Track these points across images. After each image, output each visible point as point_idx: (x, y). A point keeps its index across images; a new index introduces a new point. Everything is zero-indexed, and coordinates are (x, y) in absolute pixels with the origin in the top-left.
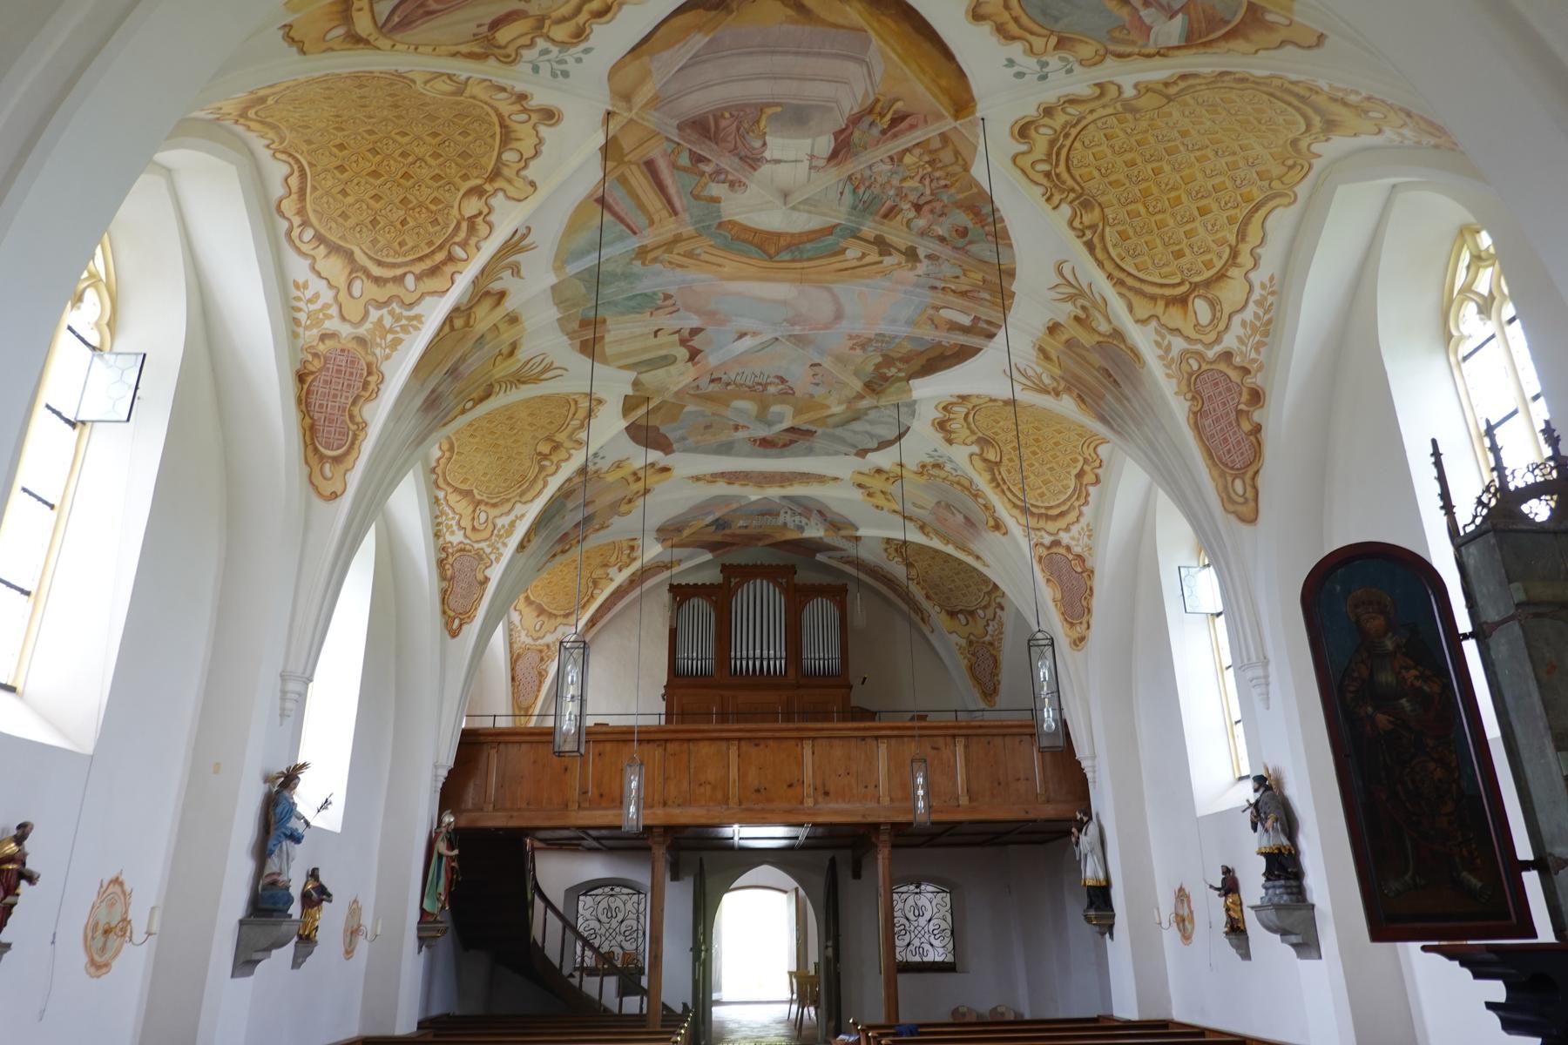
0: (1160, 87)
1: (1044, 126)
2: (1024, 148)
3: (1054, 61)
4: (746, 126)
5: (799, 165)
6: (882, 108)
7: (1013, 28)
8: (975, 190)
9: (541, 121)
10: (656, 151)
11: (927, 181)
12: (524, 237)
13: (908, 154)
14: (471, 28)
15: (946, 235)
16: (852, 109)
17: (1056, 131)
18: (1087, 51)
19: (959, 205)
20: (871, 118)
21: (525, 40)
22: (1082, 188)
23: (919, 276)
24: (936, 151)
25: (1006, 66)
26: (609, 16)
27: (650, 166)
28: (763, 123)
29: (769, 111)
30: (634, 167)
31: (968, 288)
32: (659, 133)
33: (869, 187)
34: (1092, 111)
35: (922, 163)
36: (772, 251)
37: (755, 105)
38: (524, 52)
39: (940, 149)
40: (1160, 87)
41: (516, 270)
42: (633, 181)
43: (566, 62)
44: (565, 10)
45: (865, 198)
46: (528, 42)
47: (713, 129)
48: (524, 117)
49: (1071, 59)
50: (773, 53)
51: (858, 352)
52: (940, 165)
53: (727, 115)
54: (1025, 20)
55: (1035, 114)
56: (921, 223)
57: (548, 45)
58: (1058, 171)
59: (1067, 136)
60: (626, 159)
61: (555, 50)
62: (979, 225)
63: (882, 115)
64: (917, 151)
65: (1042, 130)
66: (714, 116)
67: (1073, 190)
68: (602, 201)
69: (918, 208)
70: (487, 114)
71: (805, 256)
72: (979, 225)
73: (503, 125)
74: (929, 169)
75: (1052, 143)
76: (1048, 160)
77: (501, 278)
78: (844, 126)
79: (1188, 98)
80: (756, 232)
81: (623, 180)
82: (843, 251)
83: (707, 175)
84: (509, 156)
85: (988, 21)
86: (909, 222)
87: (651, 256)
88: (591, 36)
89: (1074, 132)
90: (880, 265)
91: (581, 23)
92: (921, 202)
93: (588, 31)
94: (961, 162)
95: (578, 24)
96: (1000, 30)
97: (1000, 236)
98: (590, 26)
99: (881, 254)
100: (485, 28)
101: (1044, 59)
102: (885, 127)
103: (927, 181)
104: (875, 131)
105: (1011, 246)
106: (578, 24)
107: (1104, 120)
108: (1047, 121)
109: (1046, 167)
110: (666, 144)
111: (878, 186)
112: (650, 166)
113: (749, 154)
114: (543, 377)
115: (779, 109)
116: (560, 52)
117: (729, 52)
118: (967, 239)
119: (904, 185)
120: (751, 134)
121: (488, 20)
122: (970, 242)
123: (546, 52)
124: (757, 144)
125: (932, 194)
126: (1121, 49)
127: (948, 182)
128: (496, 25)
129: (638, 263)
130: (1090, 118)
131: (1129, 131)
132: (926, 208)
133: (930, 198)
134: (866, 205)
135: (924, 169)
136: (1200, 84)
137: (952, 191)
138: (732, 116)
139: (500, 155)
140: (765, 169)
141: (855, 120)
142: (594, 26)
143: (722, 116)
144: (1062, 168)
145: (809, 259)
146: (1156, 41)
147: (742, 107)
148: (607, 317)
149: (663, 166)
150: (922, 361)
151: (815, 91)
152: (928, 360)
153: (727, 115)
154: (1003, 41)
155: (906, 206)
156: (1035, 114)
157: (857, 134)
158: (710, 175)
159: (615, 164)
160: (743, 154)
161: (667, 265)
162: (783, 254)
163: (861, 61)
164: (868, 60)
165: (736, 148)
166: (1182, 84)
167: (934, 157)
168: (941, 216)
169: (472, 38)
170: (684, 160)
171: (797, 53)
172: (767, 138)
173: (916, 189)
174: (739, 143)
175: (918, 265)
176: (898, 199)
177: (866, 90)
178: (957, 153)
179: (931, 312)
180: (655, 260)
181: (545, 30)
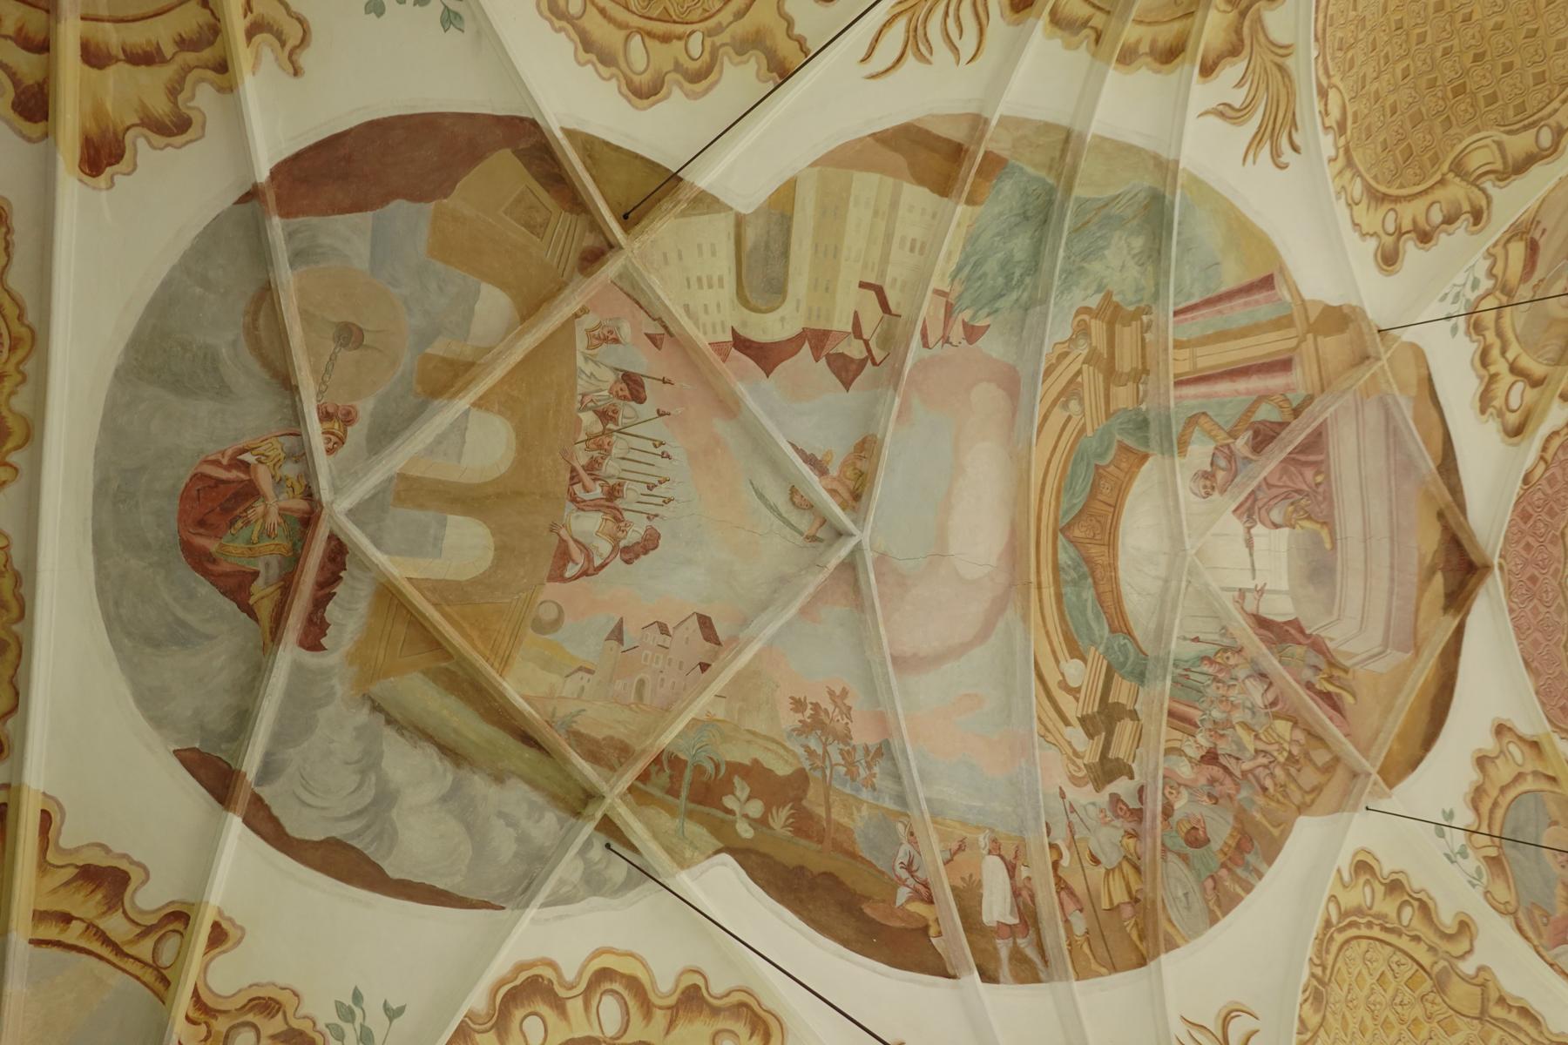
0: (1494, 995)
1: (1373, 891)
2: (1346, 876)
3: (1472, 863)
4: (1303, 502)
5: (1249, 574)
6: (1339, 678)
7: (1485, 806)
8: (1276, 832)
9: (1381, 246)
10: (1299, 380)
11: (1262, 760)
12: (1276, 154)
13: (1290, 724)
14: (1548, 223)
15: (1177, 816)
16: (1332, 640)
17: (1370, 908)
18: (1502, 892)
19: (1241, 817)
20: (1323, 666)
21: (1498, 270)
22: (1330, 979)
23: (1063, 796)
24: (1311, 760)
25: (1444, 812)
26: (1477, 363)
27: (1283, 365)
28: (1307, 524)
29: (1324, 533)
30: (1293, 343)
31: (1078, 886)
32: (1323, 390)
33: (1216, 679)
34: (1417, 939)
35: (1286, 746)
36: (1077, 533)
37: (1331, 515)
38: (1488, 263)
39: (1315, 764)
40: (1494, 995)
41: (1230, 113)
42: (1273, 336)
43: (1453, 303)
44: (1506, 322)
45: (1193, 676)
46: (1494, 271)
47: (1302, 458)
48: (1391, 228)
49: (1484, 880)
50: (1392, 539)
51: (790, 720)
52: (1293, 771)
53: (1319, 479)
54: (1499, 813)
55: (1386, 872)
56: (1185, 770)
57: (1481, 291)
58: (1335, 935)
59: (1370, 925)
60: (1310, 336)
61: (1472, 296)
62: (1222, 858)
63: (1330, 679)
64: (1300, 735)
65: (1368, 890)
66: (1322, 462)
67: (1324, 969)
68: (1267, 283)
69: (1211, 757)
70: (1402, 186)
71: (1068, 590)
72: (1222, 858)
73: (1385, 198)
74: (1281, 759)
75: (1359, 911)
76: (1343, 915)
77: (1239, 85)
78: (1308, 632)
79: (1498, 1034)
80: (1116, 507)
81: (1282, 323)
82: (1076, 652)
83: (1230, 441)
84: (1357, 189)
85: (1481, 776)
86: (1180, 752)
87: (1098, 328)
88: (1468, 339)
89: (1376, 932)
90: (1061, 725)
91: (1487, 333)
92: (1223, 760)
93: (1475, 337)
94: (1308, 798)
95: (1487, 329)
96: (1478, 793)
97: (1221, 903)
98: (1478, 341)
99: (1083, 720)
100: (1537, 236)
101: (1469, 851)
102: (1318, 686)
103: (1262, 760)
104: (1308, 674)
105: (1214, 921)
106: (1487, 329)
107: (1404, 959)
108: (1380, 889)
109: (1334, 919)
110: (1302, 393)
111: (1221, 692)
112: (1283, 365)
113: (1260, 504)
114: (900, 26)
115: (1328, 546)
116: (1468, 301)
117: (1394, 489)
118: (1189, 850)
119: (1238, 727)
120: (1291, 508)
121: (1542, 242)
122: (1185, 858)
123: (1475, 286)
124: (1276, 515)
125: (1244, 773)
126: (1526, 926)
127: (1271, 789)
128: (1533, 248)
129: (1094, 302)
130: (1404, 943)
131: (1398, 1000)
132: (1215, 771)
133: (1238, 773)
134: (1184, 681)
135: (1280, 751)
136: (1527, 1035)
137: (1261, 800)
138: (1318, 485)
139: (1363, 179)
140: (1237, 526)
141: (1317, 646)
142: (1476, 345)
143: (1318, 473)
144: (1339, 938)
145: (1059, 597)
146: (1557, 956)
147: (1329, 498)
148: (978, 209)
149: (1275, 382)
150: (815, 858)
151: (1352, 588)
152: (828, 875)
153: (1319, 479)
154: (1469, 798)
155: (1203, 740)
156: (1386, 872)
157: (1299, 650)
158: (1228, 446)
159: (1312, 320)
160: (1260, 495)
161: (1060, 349)
162: (1072, 551)
163: (1386, 643)
164: (1389, 651)
165: (1270, 486)
166: (1513, 1017)
167: (1302, 760)
168: (1210, 796)
169: (1537, 219)
170: (1266, 413)
171: (1392, 567)
172: (1286, 531)
173: (1241, 746)
174: (1275, 491)
175: (1090, 787)
176: (1209, 725)
177: (1357, 655)
178: (1317, 789)
179: (983, 840)
180: (1083, 331)
181: (1498, 293)
